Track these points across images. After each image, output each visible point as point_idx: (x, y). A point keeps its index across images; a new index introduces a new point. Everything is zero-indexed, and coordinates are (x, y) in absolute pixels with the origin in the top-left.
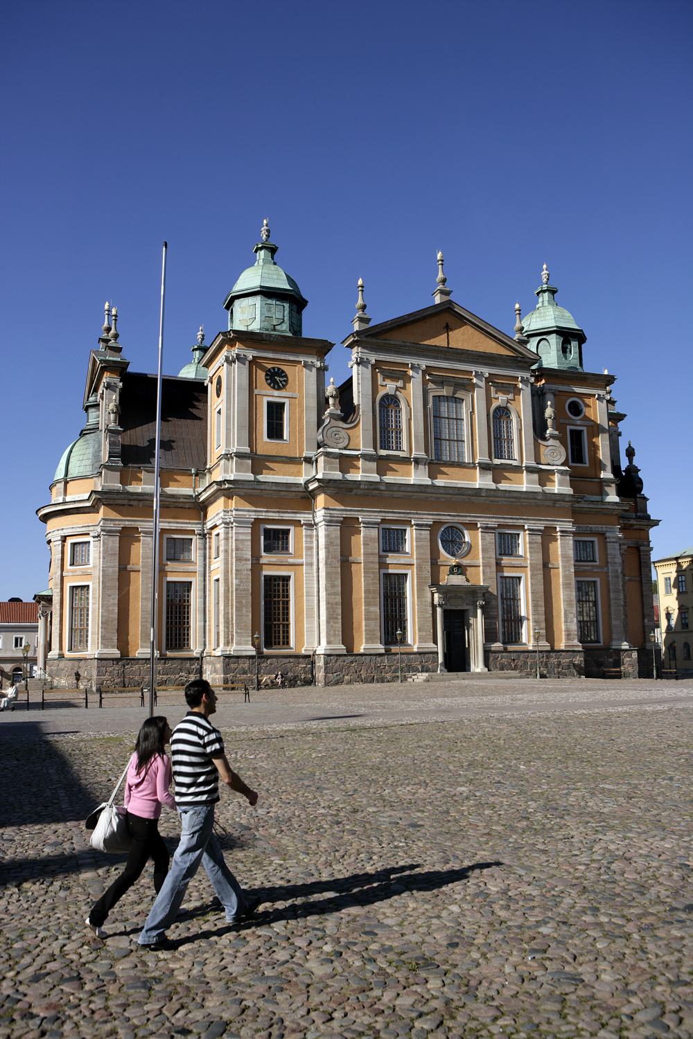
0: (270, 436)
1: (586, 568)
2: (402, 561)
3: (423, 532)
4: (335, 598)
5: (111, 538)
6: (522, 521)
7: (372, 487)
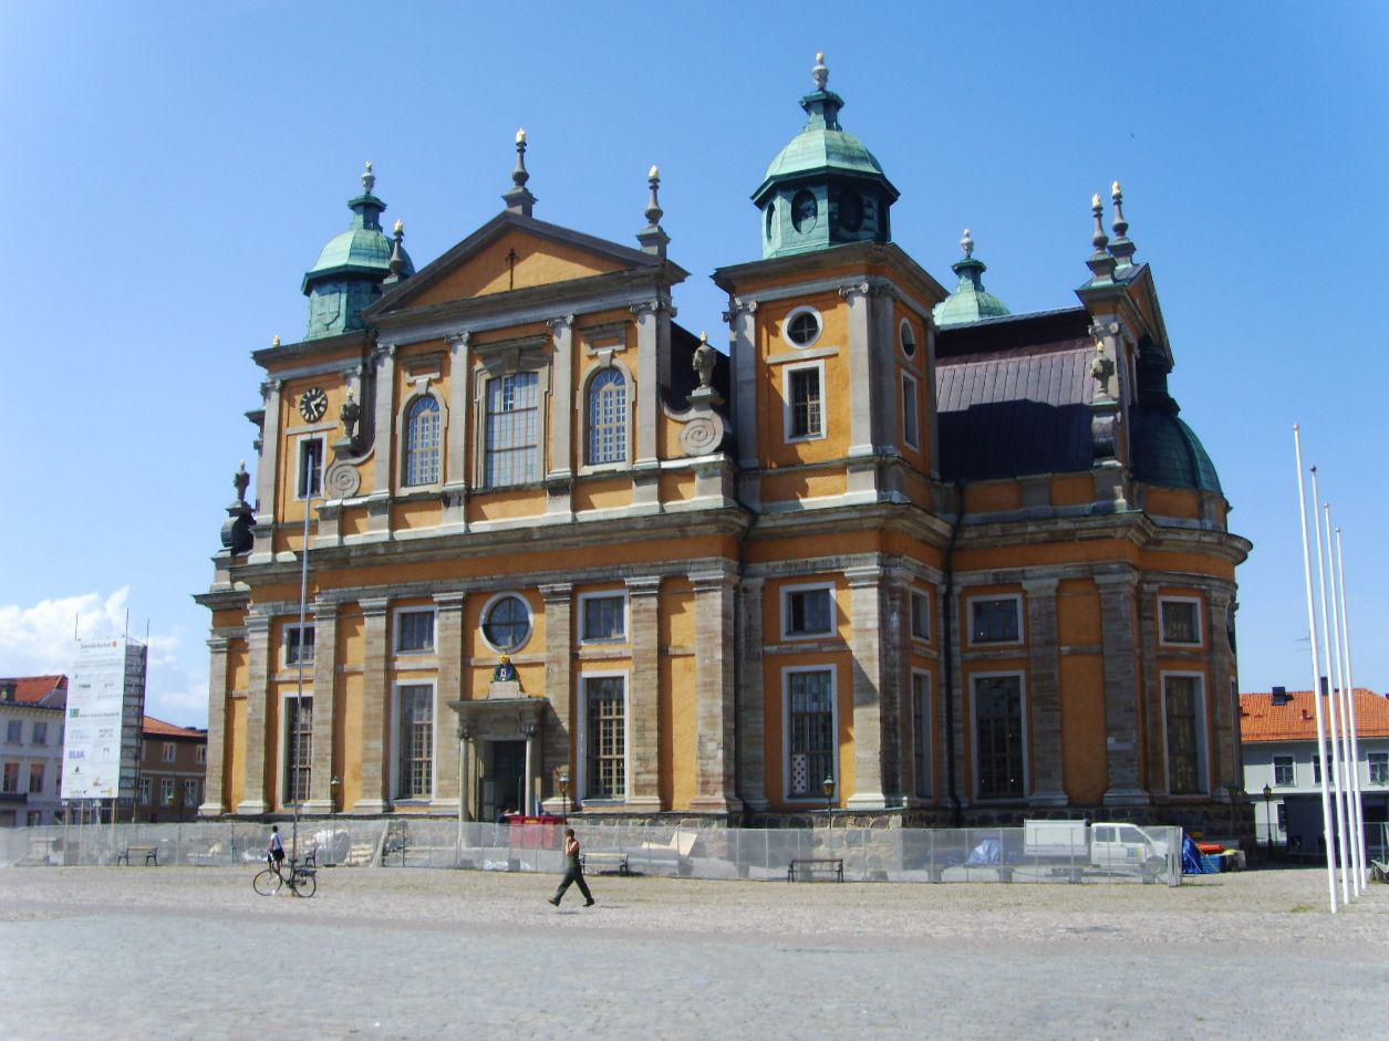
1: (808, 646)
3: (451, 614)
7: (366, 552)
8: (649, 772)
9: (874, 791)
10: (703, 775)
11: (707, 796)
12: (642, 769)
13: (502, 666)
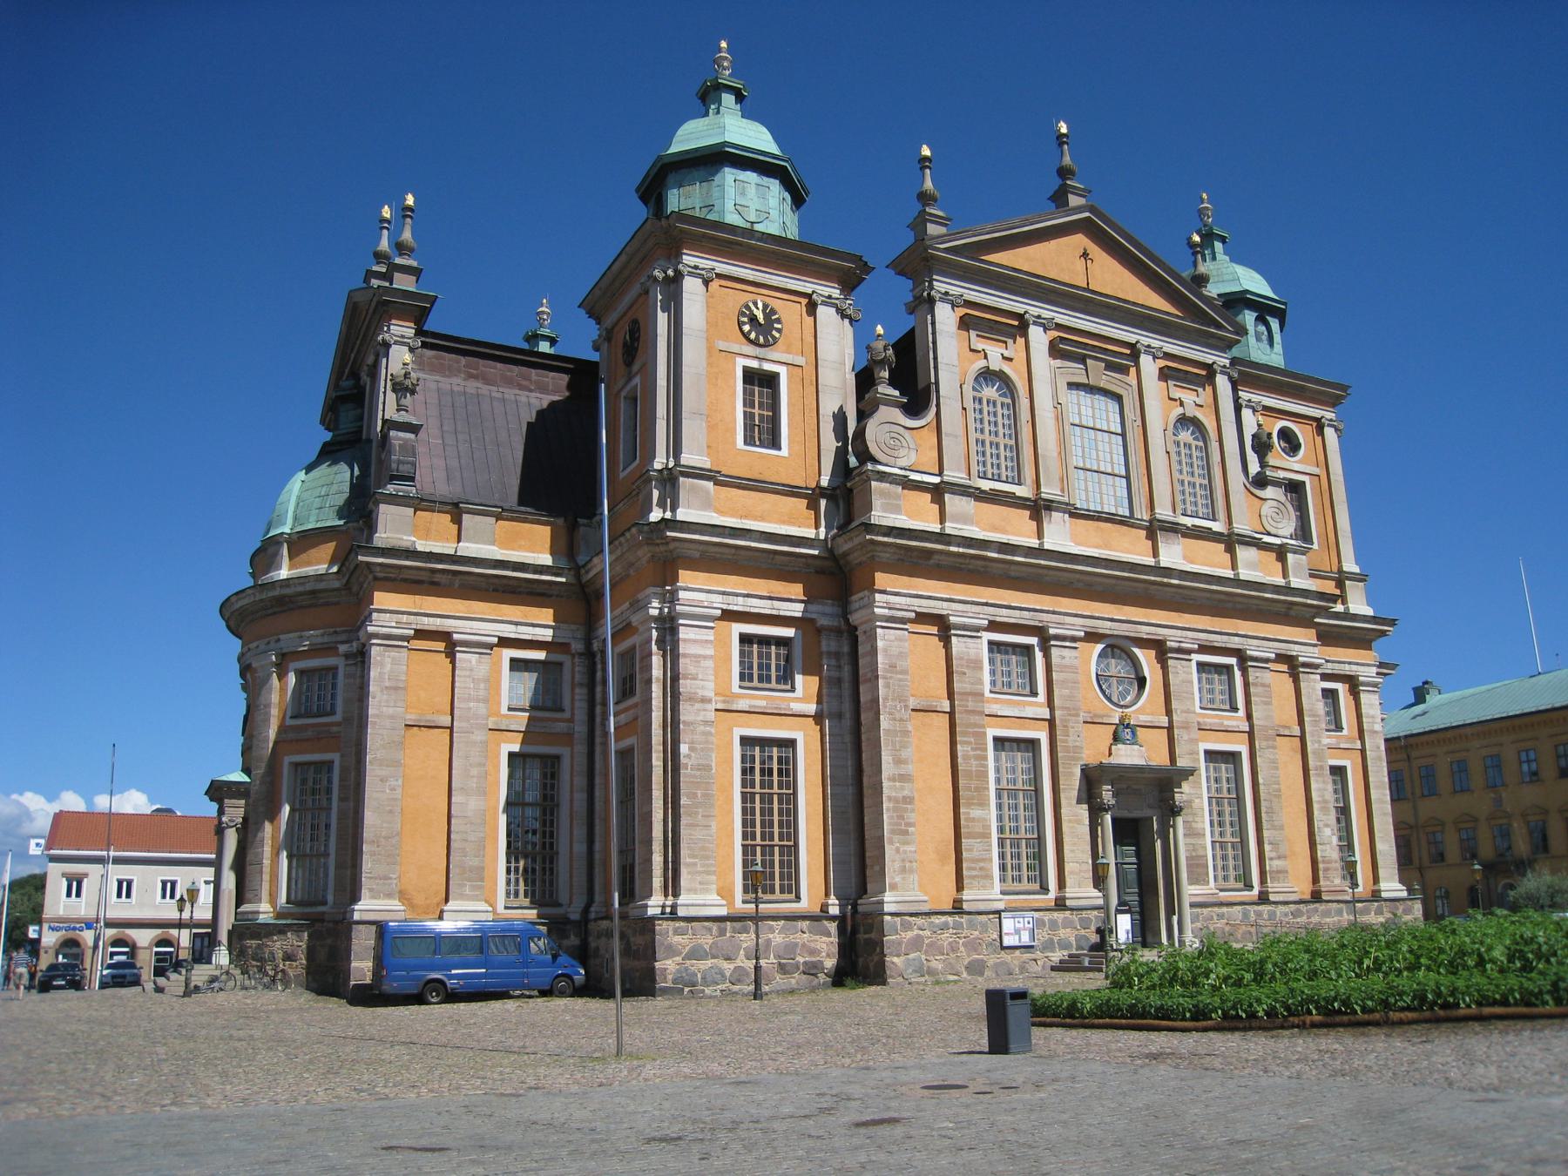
0: (749, 440)
2: (1029, 712)
3: (1066, 652)
4: (902, 788)
5: (394, 653)
6: (1237, 639)
8: (1279, 858)
9: (1389, 880)
10: (1324, 862)
11: (1328, 883)
12: (1273, 854)
13: (1128, 726)
